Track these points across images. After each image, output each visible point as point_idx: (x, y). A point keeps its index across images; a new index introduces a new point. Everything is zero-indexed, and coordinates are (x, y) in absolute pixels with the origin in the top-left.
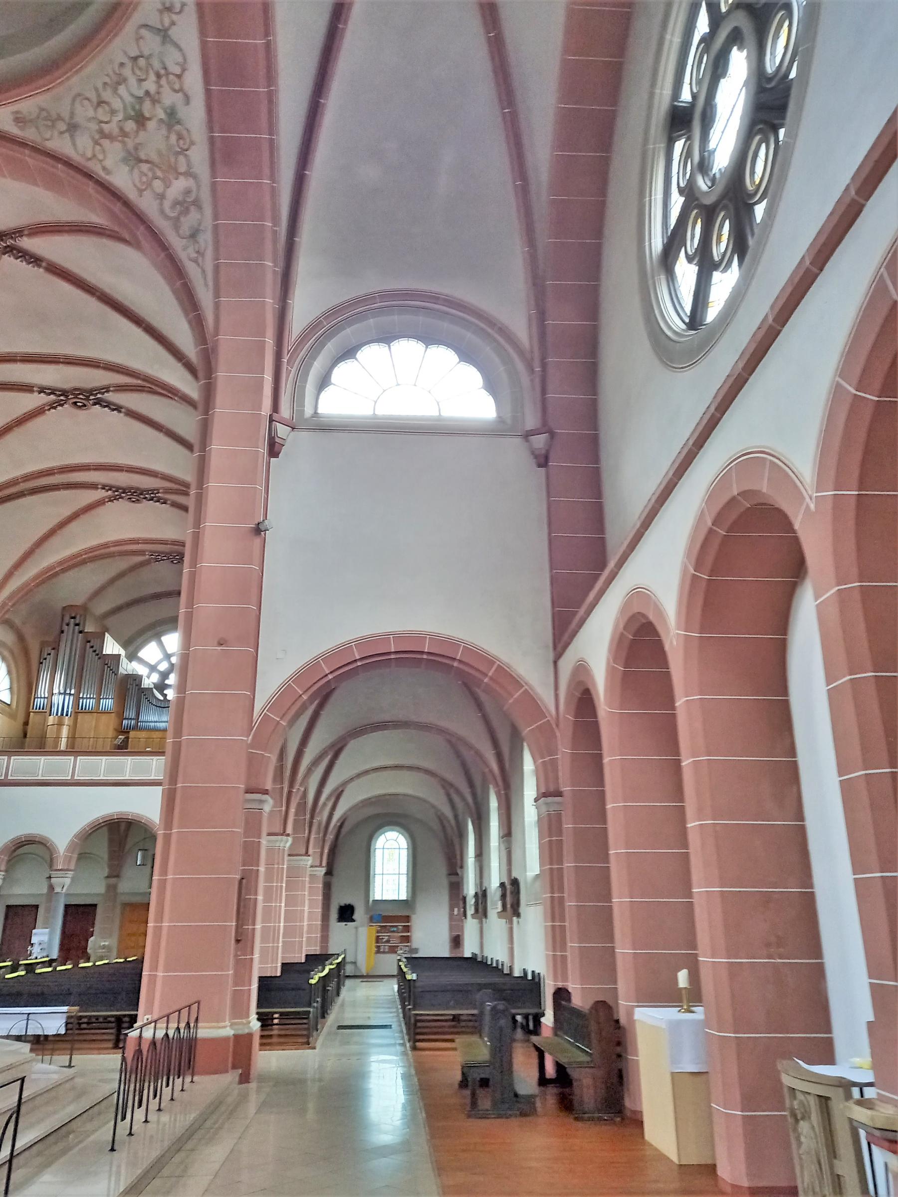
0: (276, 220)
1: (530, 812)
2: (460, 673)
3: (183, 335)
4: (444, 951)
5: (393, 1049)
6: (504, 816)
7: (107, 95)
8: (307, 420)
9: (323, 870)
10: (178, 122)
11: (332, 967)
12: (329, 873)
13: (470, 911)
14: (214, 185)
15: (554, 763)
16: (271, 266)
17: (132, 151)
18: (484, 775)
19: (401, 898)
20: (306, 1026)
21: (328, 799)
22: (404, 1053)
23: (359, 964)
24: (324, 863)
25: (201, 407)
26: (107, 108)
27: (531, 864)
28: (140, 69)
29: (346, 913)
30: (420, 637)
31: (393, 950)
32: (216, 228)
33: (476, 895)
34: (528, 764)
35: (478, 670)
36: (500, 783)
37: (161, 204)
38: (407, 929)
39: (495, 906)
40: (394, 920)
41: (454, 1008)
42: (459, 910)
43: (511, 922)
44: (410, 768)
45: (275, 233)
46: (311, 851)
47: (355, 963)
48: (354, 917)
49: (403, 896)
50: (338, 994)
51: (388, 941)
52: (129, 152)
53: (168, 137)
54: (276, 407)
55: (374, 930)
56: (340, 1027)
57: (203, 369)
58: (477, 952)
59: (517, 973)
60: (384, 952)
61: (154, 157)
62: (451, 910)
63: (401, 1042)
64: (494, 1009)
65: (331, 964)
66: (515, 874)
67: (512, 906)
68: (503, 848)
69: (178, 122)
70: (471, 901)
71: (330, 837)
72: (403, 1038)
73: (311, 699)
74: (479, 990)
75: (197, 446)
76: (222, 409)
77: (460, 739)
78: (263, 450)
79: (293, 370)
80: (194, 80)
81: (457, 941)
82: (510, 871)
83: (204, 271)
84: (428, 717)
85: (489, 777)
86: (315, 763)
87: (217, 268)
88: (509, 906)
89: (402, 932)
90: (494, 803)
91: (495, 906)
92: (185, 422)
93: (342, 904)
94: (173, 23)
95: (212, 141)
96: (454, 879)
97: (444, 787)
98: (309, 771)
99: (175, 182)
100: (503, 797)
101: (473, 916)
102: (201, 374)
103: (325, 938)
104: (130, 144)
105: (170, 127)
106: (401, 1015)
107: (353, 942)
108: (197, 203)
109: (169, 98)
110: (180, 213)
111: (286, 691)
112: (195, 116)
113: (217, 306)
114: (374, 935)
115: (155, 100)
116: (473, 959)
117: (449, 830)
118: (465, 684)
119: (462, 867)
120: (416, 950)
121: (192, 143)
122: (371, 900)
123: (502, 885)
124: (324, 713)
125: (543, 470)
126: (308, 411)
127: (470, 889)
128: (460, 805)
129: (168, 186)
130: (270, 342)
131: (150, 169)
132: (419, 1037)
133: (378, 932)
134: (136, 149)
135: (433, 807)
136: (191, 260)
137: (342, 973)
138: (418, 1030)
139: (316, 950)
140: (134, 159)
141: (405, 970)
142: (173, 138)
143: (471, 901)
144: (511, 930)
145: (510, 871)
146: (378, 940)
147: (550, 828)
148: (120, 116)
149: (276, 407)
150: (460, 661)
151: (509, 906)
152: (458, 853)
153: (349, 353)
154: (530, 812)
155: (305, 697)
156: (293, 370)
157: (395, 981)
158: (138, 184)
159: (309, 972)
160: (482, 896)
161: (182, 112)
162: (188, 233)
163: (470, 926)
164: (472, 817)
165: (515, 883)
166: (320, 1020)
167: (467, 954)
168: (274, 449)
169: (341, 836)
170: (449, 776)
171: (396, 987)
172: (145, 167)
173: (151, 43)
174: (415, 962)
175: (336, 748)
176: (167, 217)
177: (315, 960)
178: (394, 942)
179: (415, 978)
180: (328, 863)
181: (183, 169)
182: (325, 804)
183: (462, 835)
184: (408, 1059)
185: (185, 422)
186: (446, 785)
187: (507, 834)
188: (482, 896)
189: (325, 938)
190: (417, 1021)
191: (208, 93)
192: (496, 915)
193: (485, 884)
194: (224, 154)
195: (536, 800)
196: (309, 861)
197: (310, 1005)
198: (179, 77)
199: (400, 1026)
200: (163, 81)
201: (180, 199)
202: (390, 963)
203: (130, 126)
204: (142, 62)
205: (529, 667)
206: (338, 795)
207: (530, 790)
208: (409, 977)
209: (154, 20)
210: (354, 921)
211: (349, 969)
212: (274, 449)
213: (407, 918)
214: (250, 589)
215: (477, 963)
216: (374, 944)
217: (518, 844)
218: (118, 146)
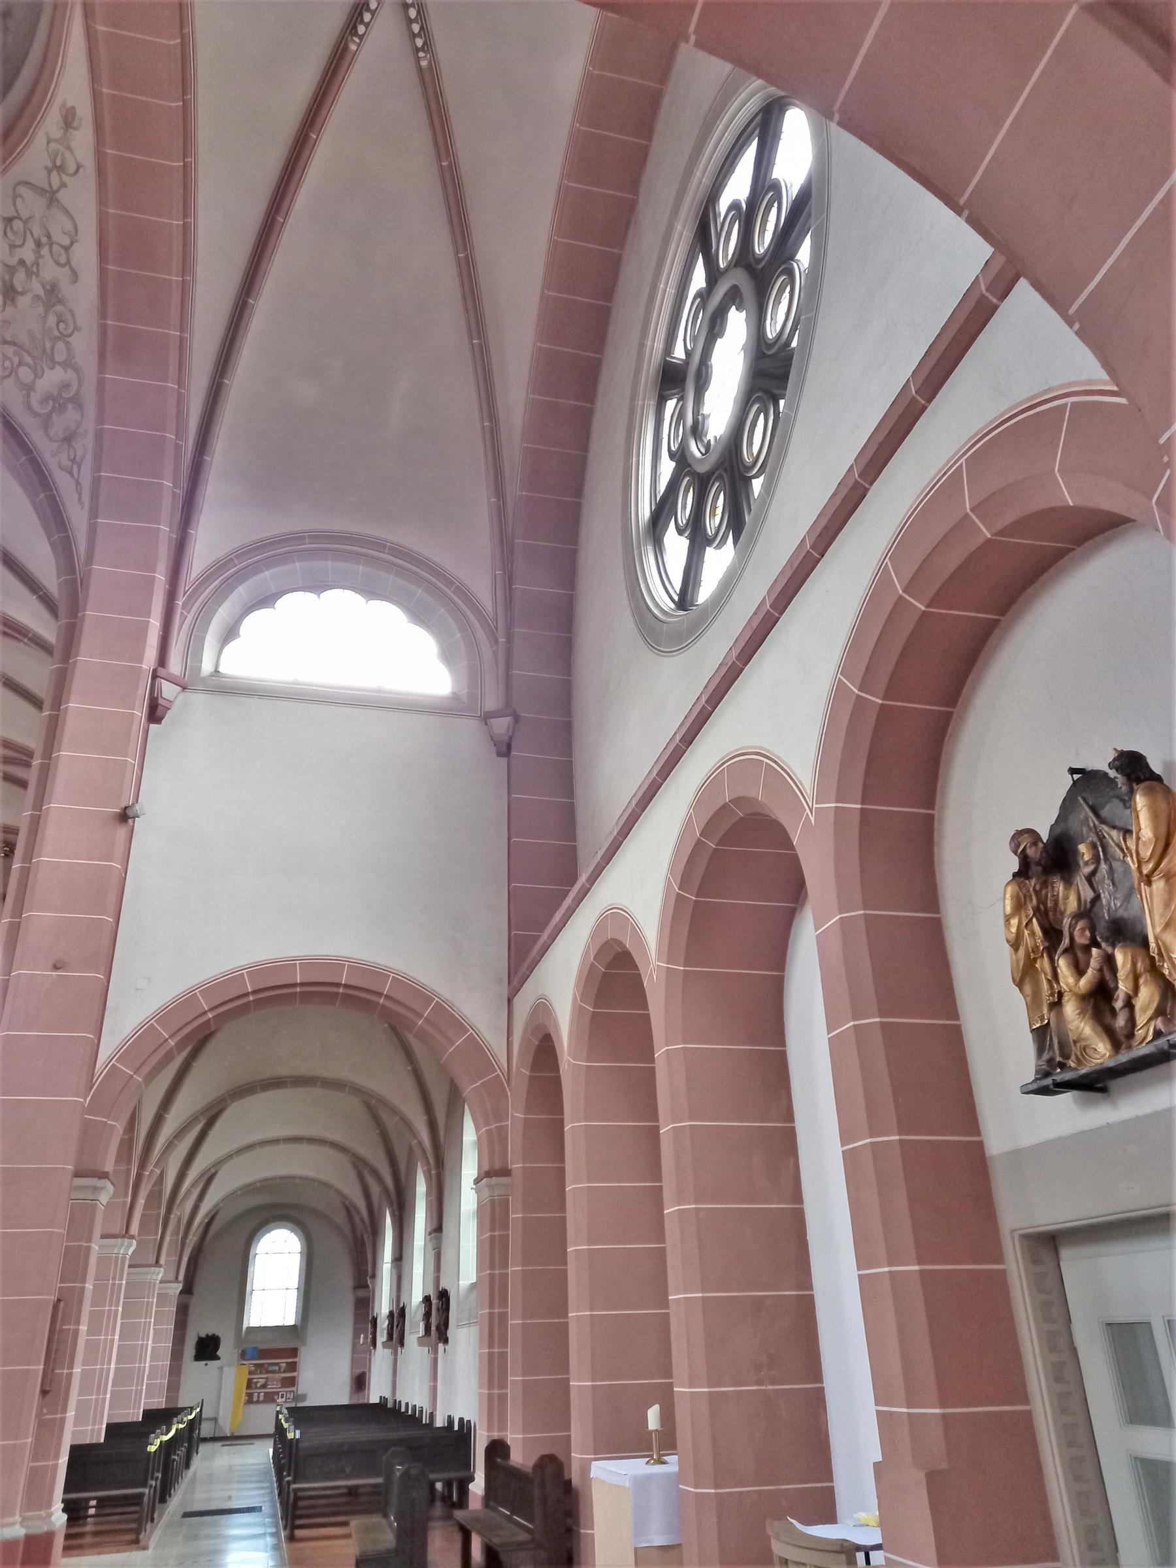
0: (180, 432)
1: (468, 1198)
2: (385, 1013)
3: (42, 561)
4: (339, 1395)
5: (260, 1543)
6: (434, 1203)
8: (203, 679)
9: (180, 1287)
10: (60, 302)
11: (181, 1426)
12: (188, 1290)
13: (382, 1337)
14: (101, 382)
15: (502, 1134)
16: (169, 487)
18: (411, 1148)
19: (287, 1324)
20: (135, 1516)
21: (194, 1185)
22: (276, 1548)
23: (220, 1421)
24: (181, 1277)
25: (58, 653)
27: (466, 1269)
28: (15, 233)
29: (207, 1349)
30: (335, 965)
31: (270, 1398)
32: (99, 435)
33: (391, 1314)
34: (469, 1134)
35: (409, 1009)
36: (431, 1160)
37: (28, 395)
38: (293, 1367)
39: (415, 1328)
40: (277, 1352)
41: (347, 1477)
42: (366, 1338)
43: (436, 1352)
44: (311, 1140)
45: (178, 448)
46: (162, 1261)
47: (215, 1420)
48: (219, 1353)
49: (290, 1320)
50: (187, 1466)
51: (264, 1386)
53: (45, 316)
54: (162, 660)
55: (245, 1372)
56: (186, 1515)
57: (67, 606)
58: (388, 1395)
59: (440, 1422)
60: (258, 1402)
61: (23, 338)
62: (356, 1336)
63: (274, 1530)
64: (406, 1475)
65: (182, 1422)
66: (444, 1284)
67: (438, 1328)
68: (430, 1247)
69: (60, 302)
70: (383, 1324)
71: (193, 1239)
72: (276, 1525)
73: (180, 1046)
74: (386, 1450)
75: (50, 704)
76: (87, 658)
77: (382, 1101)
78: (141, 713)
79: (190, 617)
80: (86, 254)
81: (360, 1382)
82: (437, 1280)
83: (78, 483)
84: (343, 1072)
85: (418, 1152)
86: (179, 1134)
87: (96, 481)
88: (433, 1328)
89: (284, 1372)
90: (421, 1187)
91: (415, 1328)
92: (36, 673)
93: (203, 1335)
94: (63, 185)
95: (103, 331)
96: (361, 1293)
97: (355, 1166)
98: (170, 1146)
99: (48, 372)
100: (434, 1177)
101: (385, 1345)
102: (62, 610)
103: (174, 1387)
105: (48, 307)
106: (276, 1492)
107: (214, 1389)
108: (77, 401)
109: (50, 271)
110: (53, 410)
111: (146, 1033)
112: (83, 297)
113: (93, 529)
114: (246, 1376)
115: (32, 272)
116: (382, 1405)
117: (360, 1227)
118: (393, 1028)
119: (374, 1276)
120: (303, 1397)
121: (76, 328)
122: (245, 1326)
123: (427, 1299)
124: (198, 1067)
125: (504, 760)
126: (207, 667)
127: (383, 1307)
128: (375, 1189)
129: (38, 375)
130: (161, 578)
131: (15, 353)
132: (299, 1522)
133: (250, 1373)
135: (338, 1192)
136: (62, 468)
137: (195, 1435)
138: (299, 1512)
139: (159, 1402)
141: (286, 1425)
142: (52, 320)
143: (383, 1324)
144: (435, 1360)
145: (437, 1280)
146: (250, 1384)
147: (493, 1220)
149: (162, 660)
150: (387, 997)
151: (433, 1328)
152: (369, 1256)
153: (266, 600)
154: (468, 1198)
155: (172, 1043)
156: (190, 617)
157: (271, 1442)
159: (147, 1435)
160: (399, 1316)
161: (66, 290)
162: (61, 436)
163: (381, 1357)
164: (391, 1205)
165: (444, 1296)
166: (157, 1505)
167: (374, 1399)
168: (155, 713)
169: (210, 1235)
170: (362, 1151)
171: (271, 1451)
173: (31, 204)
174: (300, 1415)
175: (211, 1113)
176: (36, 415)
177: (156, 1418)
178: (273, 1387)
179: (298, 1436)
180: (186, 1277)
181: (60, 357)
182: (188, 1192)
183: (376, 1231)
184: (281, 1557)
185: (36, 673)
186: (360, 1165)
187: (437, 1228)
188: (399, 1316)
189: (174, 1387)
190: (297, 1499)
191: (103, 272)
192: (416, 1341)
193: (404, 1299)
194: (117, 346)
195: (477, 1181)
196: (159, 1274)
197: (144, 1484)
198: (67, 249)
199: (274, 1506)
200: (45, 251)
201: (55, 393)
202: (264, 1417)
204: (17, 225)
205: (478, 1009)
206: (209, 1179)
207: (469, 1170)
208: (290, 1436)
209: (40, 178)
210: (218, 1358)
211: (206, 1429)
212: (155, 713)
213: (294, 1352)
214: (108, 893)
215: (387, 1412)
216: (245, 1391)
217: (449, 1246)
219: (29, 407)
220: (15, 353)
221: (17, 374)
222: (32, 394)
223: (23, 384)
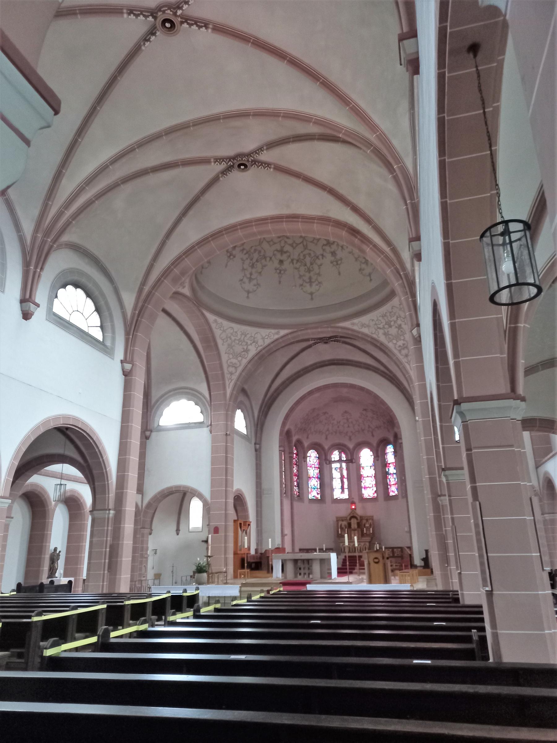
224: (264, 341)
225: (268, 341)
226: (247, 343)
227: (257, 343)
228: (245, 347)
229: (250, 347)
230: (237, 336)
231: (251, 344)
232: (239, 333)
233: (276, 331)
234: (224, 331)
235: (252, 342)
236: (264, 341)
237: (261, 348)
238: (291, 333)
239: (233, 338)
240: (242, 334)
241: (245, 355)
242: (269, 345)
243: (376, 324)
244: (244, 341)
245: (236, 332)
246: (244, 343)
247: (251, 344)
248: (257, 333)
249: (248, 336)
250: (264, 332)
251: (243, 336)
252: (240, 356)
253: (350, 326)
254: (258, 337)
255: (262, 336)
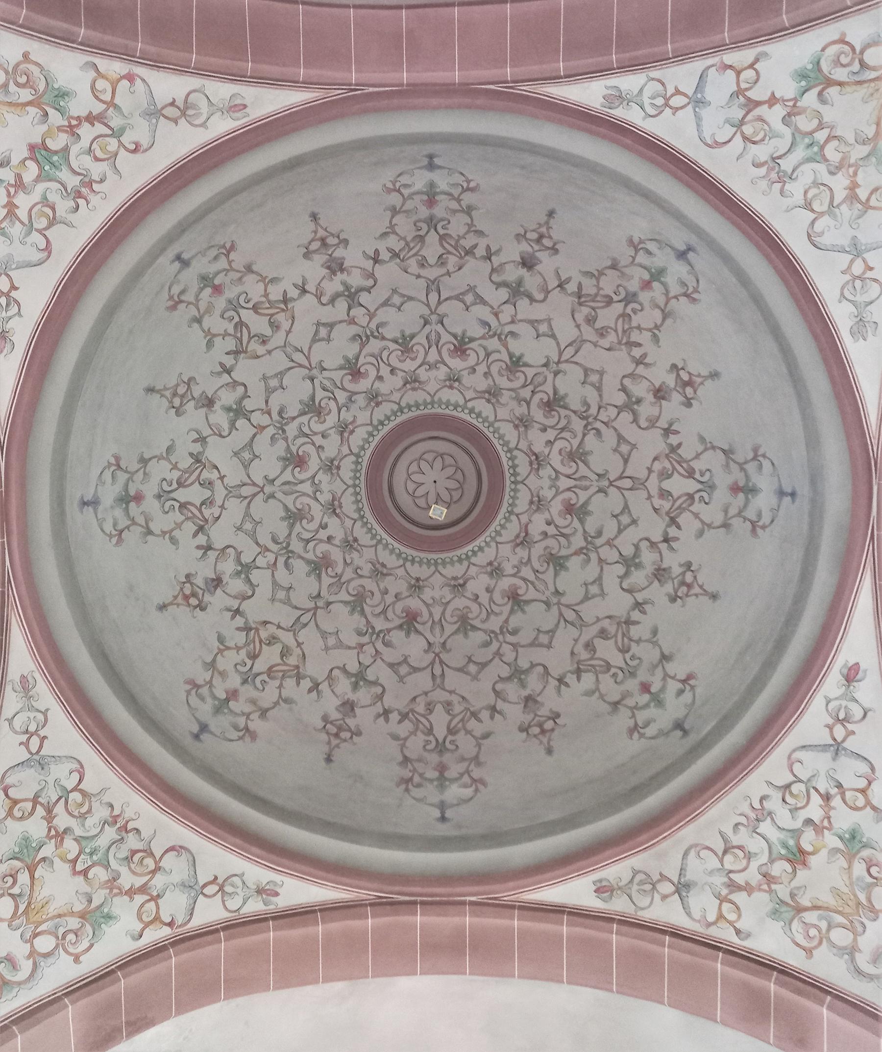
7: (742, 838)
17: (788, 900)
26: (740, 853)
52: (783, 902)
104: (783, 891)
131: (820, 918)
134: (792, 896)
140: (790, 909)
148: (764, 859)
158: (804, 943)
172: (811, 917)
203: (780, 868)
218: (761, 897)
219: (859, 972)
220: (820, 918)
221: (829, 940)
222: (857, 955)
223: (841, 948)
224: (700, 86)
225: (682, 76)
226: (786, 120)
227: (739, 92)
228: (810, 99)
229: (787, 89)
230: (816, 184)
231: (773, 101)
232: (796, 189)
233: (619, 113)
234: (856, 250)
235: (762, 110)
236: (700, 86)
237: (730, 58)
238: (554, 78)
239: (840, 184)
240: (784, 178)
241: (837, 63)
242: (682, 56)
243: (117, 134)
244: (797, 132)
245: (808, 206)
246: (804, 123)
247: (773, 101)
248: (717, 145)
249: (762, 152)
250: (676, 130)
251: (787, 165)
252: (863, 65)
253: (248, 92)
254: (715, 122)
255: (698, 118)
